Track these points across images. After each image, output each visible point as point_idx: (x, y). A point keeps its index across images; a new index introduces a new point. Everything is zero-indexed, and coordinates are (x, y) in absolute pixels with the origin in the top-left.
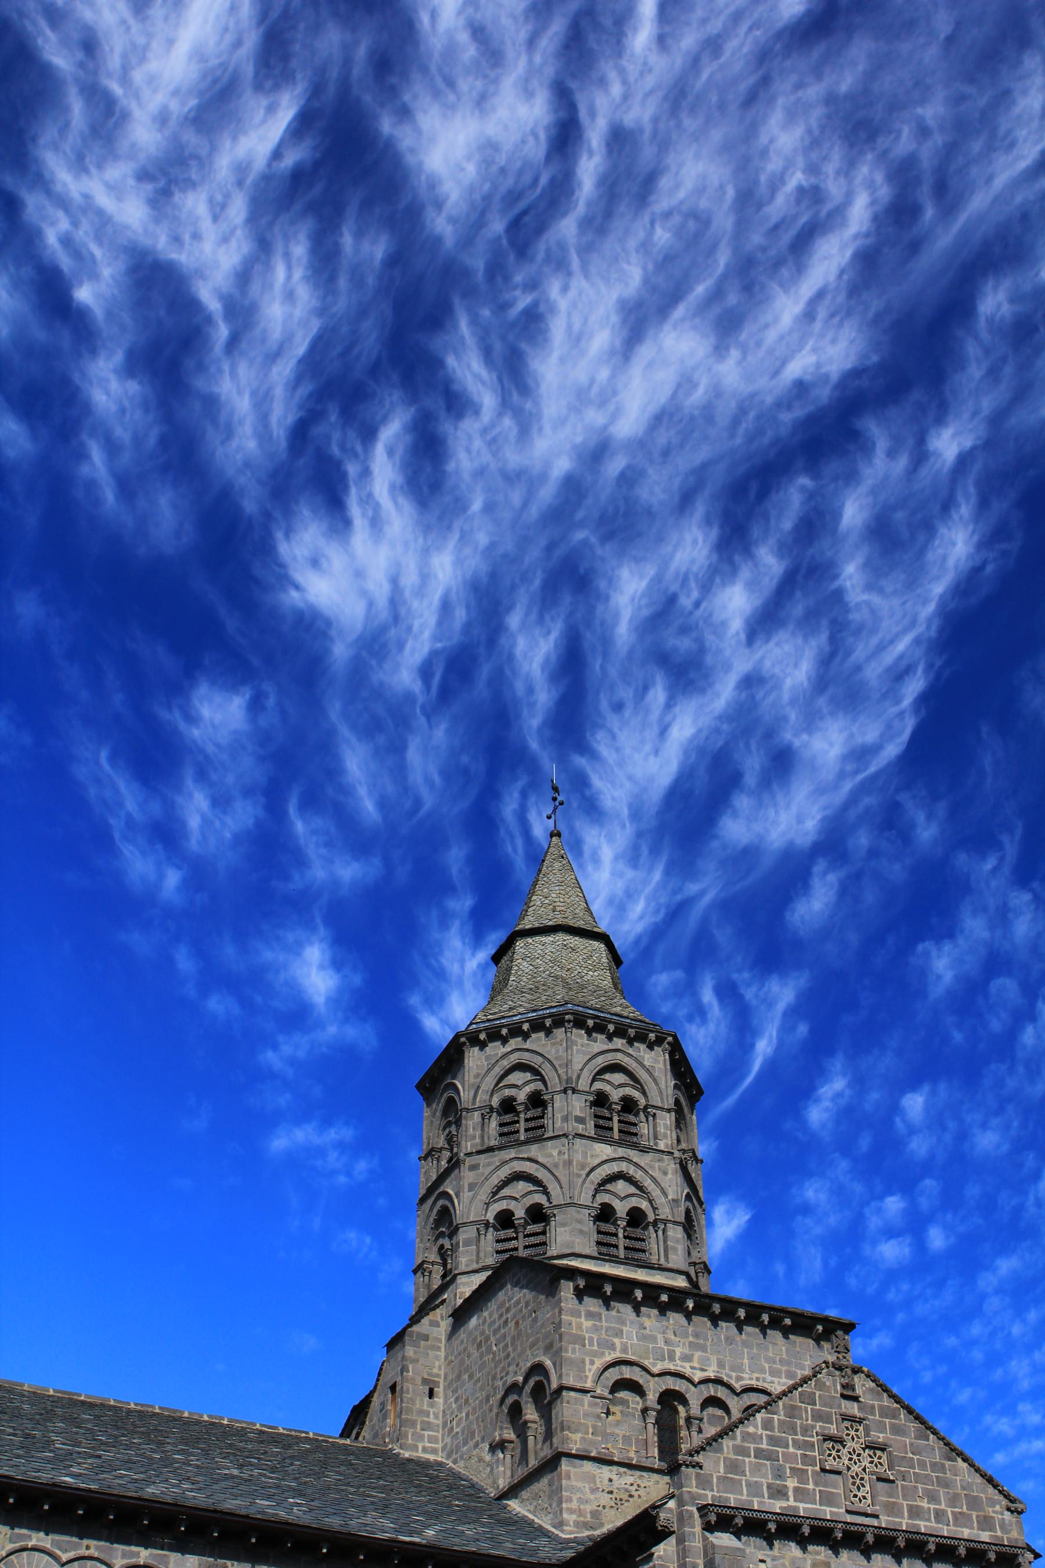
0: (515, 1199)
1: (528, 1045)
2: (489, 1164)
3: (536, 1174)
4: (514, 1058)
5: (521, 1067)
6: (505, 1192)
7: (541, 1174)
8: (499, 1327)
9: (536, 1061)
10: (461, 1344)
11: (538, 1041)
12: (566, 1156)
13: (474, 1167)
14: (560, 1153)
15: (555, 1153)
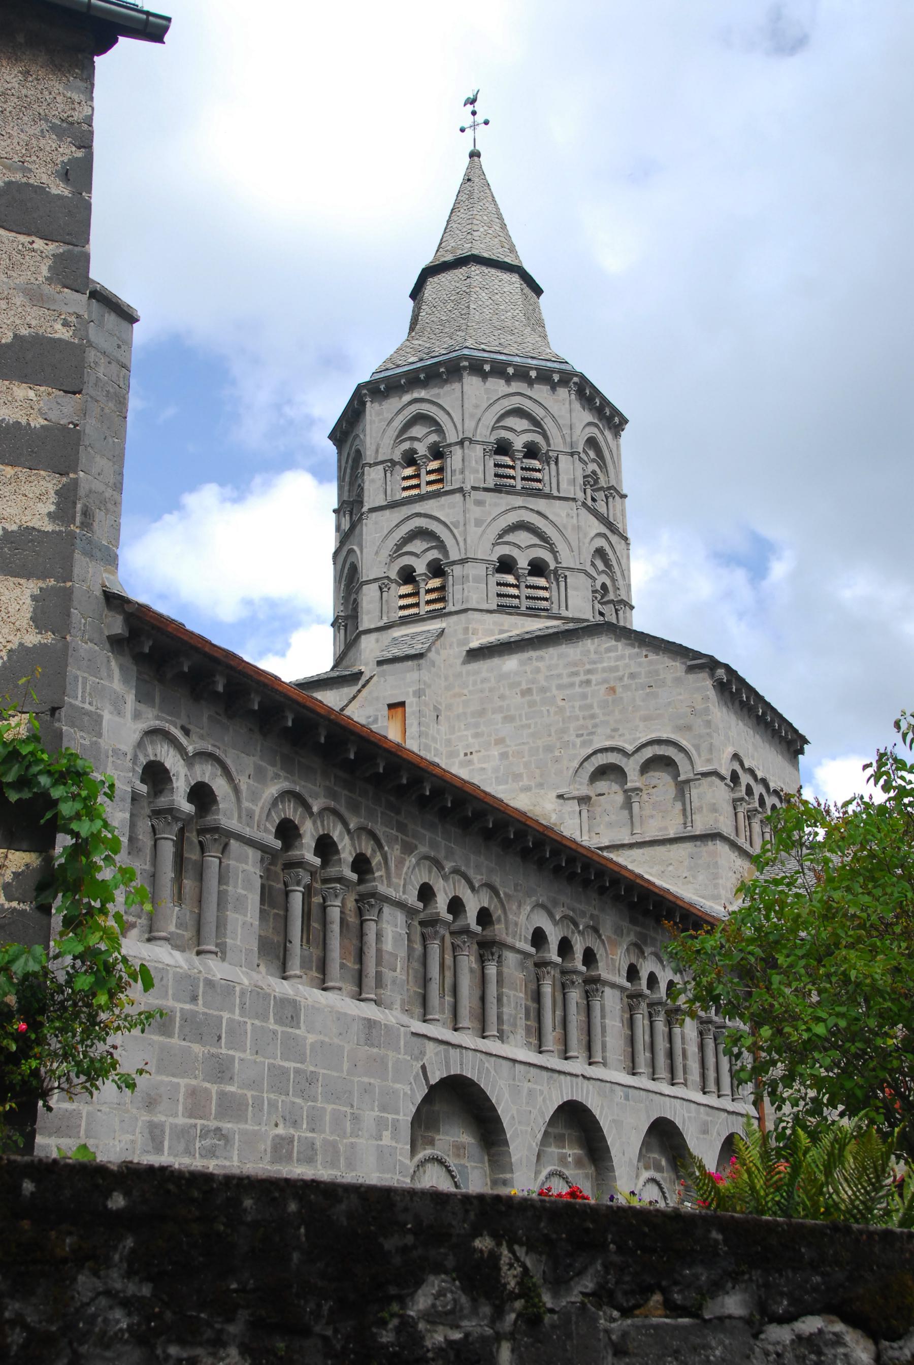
0: (519, 547)
1: (528, 392)
2: (496, 505)
3: (544, 529)
4: (516, 402)
5: (519, 412)
6: (509, 538)
7: (550, 531)
8: (572, 685)
9: (539, 412)
10: (482, 681)
11: (541, 392)
12: (575, 521)
13: (479, 503)
14: (568, 515)
15: (564, 514)
